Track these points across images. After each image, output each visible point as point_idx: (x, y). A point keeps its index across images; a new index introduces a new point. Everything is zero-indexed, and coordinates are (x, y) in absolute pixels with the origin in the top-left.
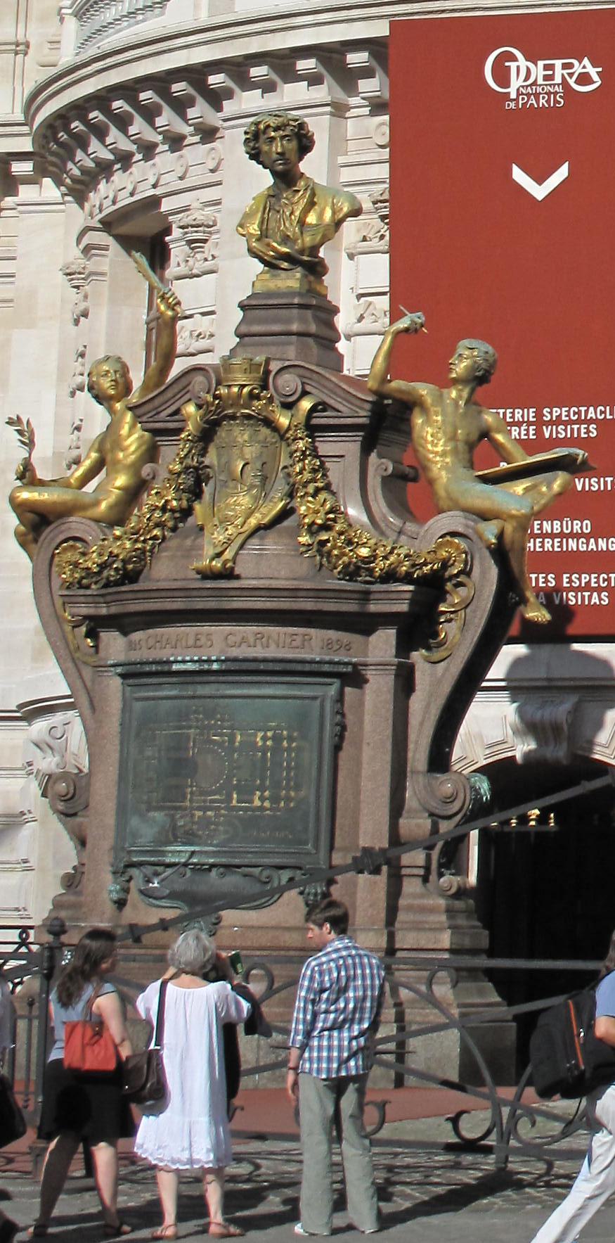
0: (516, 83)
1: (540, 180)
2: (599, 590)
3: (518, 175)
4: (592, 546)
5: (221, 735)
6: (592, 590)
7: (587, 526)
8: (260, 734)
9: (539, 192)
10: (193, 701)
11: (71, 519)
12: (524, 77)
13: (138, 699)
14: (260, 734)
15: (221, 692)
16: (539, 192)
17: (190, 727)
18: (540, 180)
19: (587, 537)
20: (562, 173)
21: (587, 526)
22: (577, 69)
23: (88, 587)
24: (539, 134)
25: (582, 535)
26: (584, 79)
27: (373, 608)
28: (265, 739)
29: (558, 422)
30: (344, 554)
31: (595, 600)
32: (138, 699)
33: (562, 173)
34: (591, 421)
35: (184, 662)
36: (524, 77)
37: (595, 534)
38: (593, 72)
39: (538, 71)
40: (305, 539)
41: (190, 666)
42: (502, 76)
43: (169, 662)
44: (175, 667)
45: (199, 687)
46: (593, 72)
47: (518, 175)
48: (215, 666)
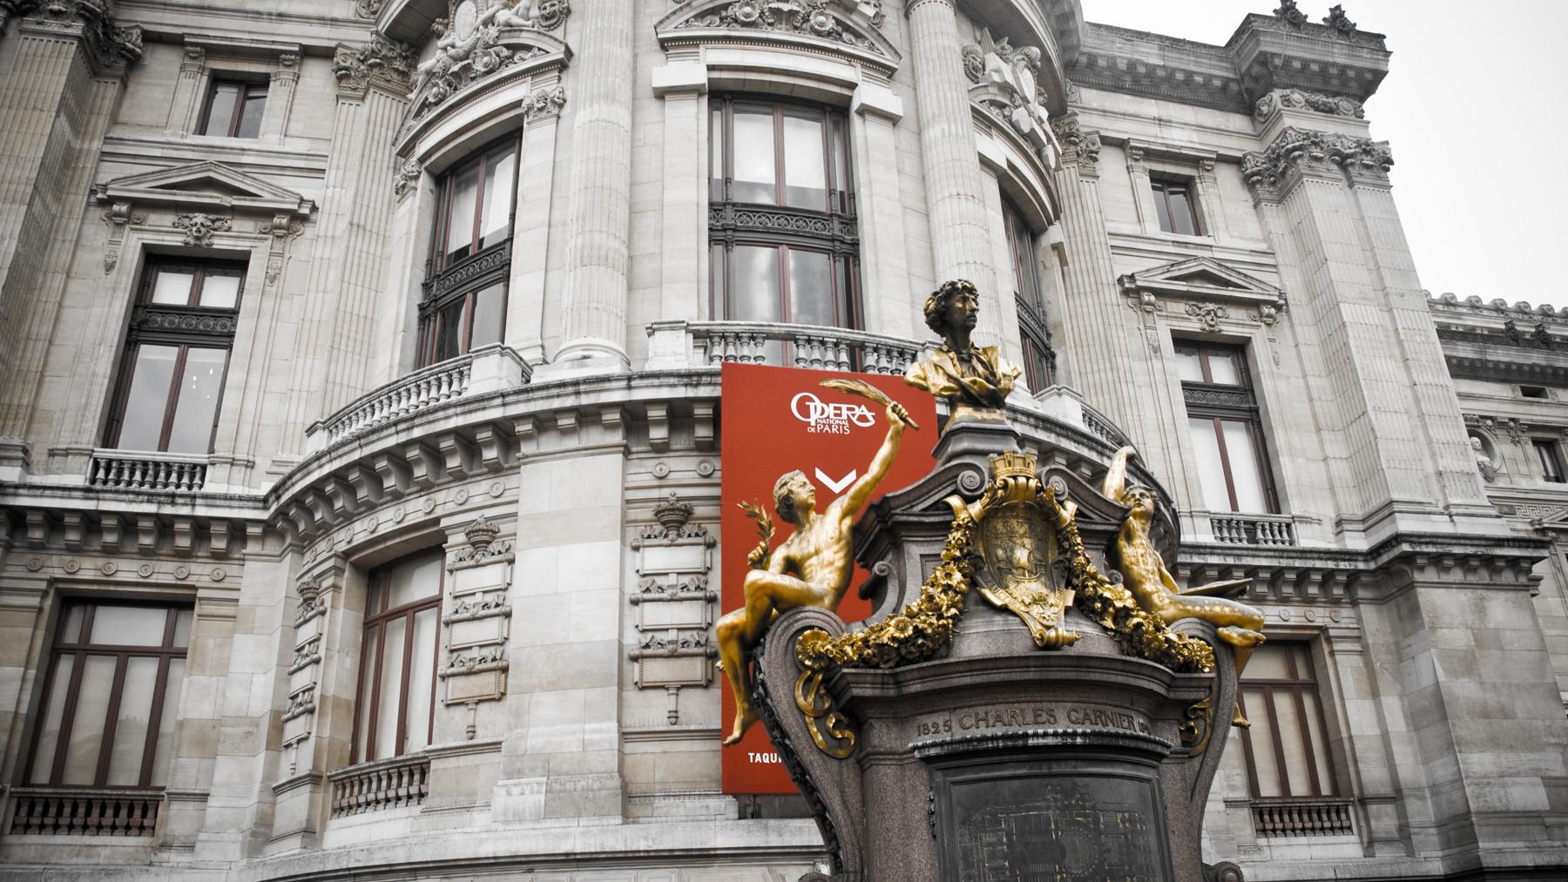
5: (1085, 816)
8: (1119, 816)
10: (1046, 781)
11: (809, 608)
13: (955, 783)
14: (1119, 816)
15: (1080, 770)
17: (1048, 808)
23: (877, 666)
28: (1123, 821)
30: (1156, 639)
32: (955, 783)
35: (1045, 735)
40: (1109, 623)
41: (1050, 741)
43: (1026, 736)
44: (1031, 742)
45: (1054, 764)
48: (1079, 740)
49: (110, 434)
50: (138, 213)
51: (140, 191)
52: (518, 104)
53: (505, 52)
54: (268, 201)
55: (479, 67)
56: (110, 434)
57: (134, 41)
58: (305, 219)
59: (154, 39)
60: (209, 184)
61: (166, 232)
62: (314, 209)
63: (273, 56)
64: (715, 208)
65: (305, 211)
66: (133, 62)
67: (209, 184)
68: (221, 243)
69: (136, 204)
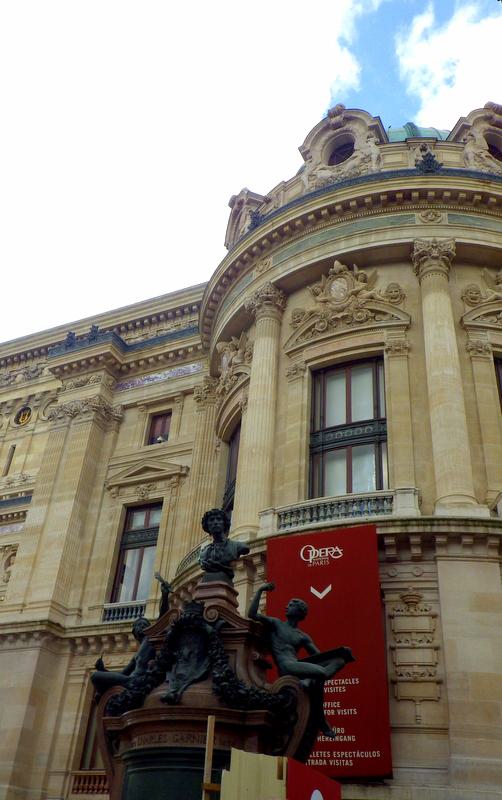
0: (311, 557)
1: (321, 591)
2: (349, 759)
3: (313, 590)
4: (345, 739)
6: (345, 759)
7: (343, 730)
9: (321, 596)
12: (315, 555)
16: (321, 596)
18: (321, 591)
19: (343, 735)
20: (329, 589)
21: (343, 730)
22: (334, 550)
24: (319, 575)
25: (341, 734)
26: (336, 554)
27: (247, 723)
29: (330, 686)
31: (347, 764)
33: (329, 589)
34: (342, 685)
36: (315, 555)
37: (346, 734)
38: (340, 551)
39: (320, 553)
42: (307, 555)
46: (340, 551)
47: (313, 590)
49: (114, 595)
50: (122, 490)
51: (121, 480)
52: (237, 406)
53: (235, 377)
54: (168, 471)
55: (227, 389)
56: (114, 595)
57: (117, 412)
58: (185, 475)
59: (125, 408)
60: (147, 469)
61: (132, 496)
62: (189, 469)
63: (171, 400)
64: (313, 434)
65: (184, 472)
66: (120, 421)
67: (147, 469)
68: (153, 496)
69: (121, 486)
